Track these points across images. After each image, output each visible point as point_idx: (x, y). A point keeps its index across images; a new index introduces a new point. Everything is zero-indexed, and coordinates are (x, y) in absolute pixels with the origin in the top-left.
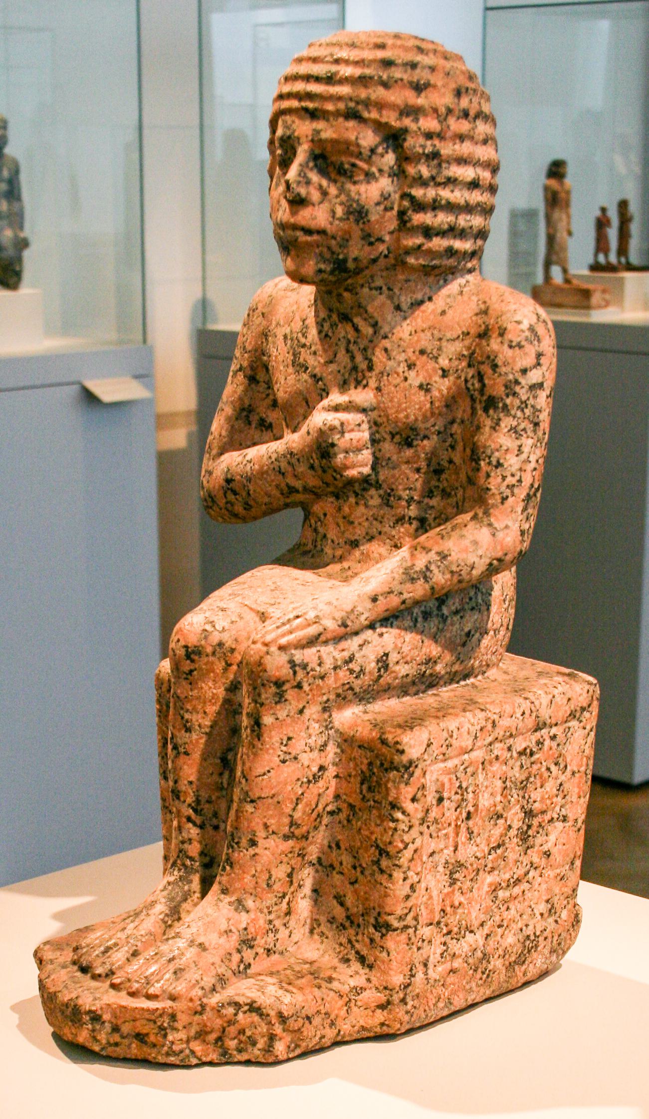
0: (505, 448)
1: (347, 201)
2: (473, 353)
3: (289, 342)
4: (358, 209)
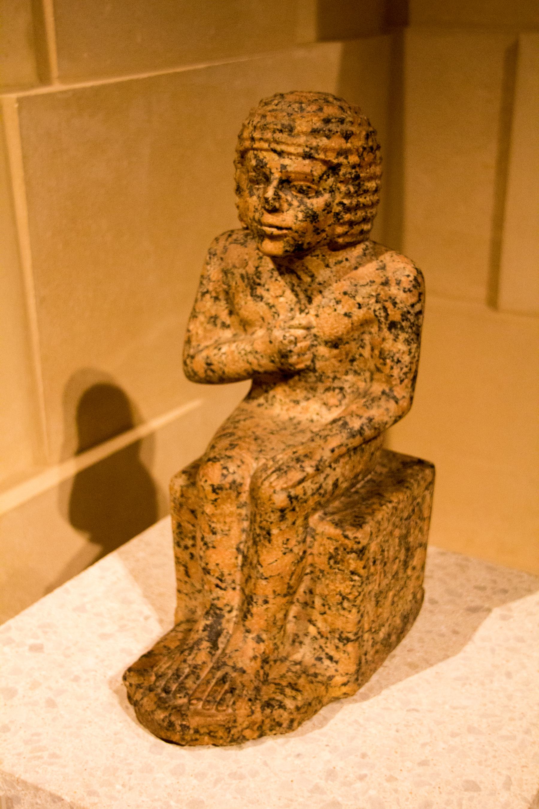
0: (402, 351)
1: (305, 210)
2: (379, 294)
3: (246, 280)
4: (312, 214)
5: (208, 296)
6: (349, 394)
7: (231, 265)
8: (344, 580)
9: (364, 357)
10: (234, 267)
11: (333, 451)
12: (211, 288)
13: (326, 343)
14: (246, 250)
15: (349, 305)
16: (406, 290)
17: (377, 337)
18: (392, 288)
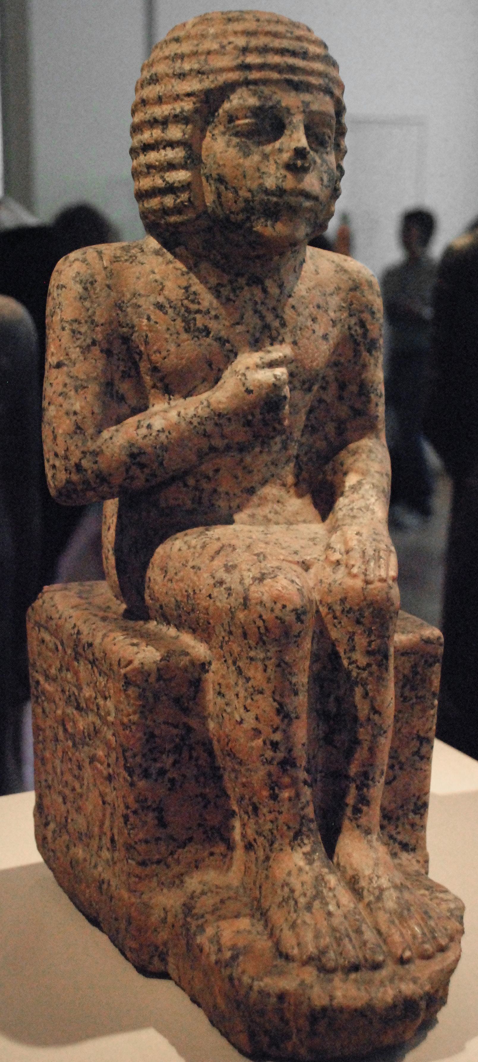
3: (170, 311)
5: (96, 350)
7: (128, 296)
12: (99, 337)
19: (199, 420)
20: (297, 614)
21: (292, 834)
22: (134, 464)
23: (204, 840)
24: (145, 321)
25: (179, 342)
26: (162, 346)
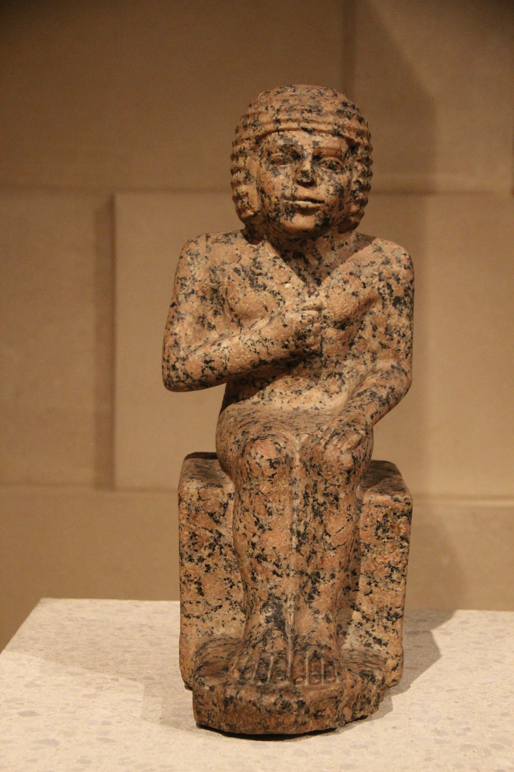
0: (406, 326)
2: (380, 274)
3: (242, 273)
5: (194, 297)
6: (348, 379)
7: (219, 263)
8: (394, 548)
9: (364, 339)
10: (224, 263)
11: (372, 417)
12: (196, 288)
13: (335, 323)
14: (235, 246)
15: (356, 284)
16: (406, 267)
17: (380, 315)
18: (394, 266)
19: (252, 342)
20: (271, 462)
21: (262, 604)
22: (207, 367)
23: (230, 609)
24: (226, 279)
25: (245, 292)
26: (235, 295)
